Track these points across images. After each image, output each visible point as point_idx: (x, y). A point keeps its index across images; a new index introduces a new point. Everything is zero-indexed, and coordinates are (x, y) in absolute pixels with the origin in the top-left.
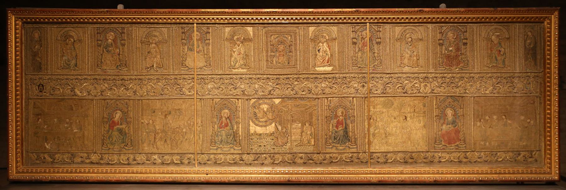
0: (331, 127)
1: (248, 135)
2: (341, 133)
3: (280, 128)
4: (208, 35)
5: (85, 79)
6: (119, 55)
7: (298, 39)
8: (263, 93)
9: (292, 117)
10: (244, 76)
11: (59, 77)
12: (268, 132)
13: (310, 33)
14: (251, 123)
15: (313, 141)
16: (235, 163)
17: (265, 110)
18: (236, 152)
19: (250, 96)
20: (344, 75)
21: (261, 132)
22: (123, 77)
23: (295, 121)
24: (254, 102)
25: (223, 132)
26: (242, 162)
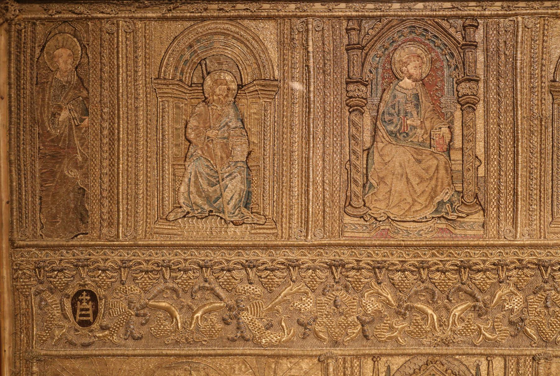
5: (291, 265)
6: (449, 149)
11: (168, 256)
22: (460, 257)
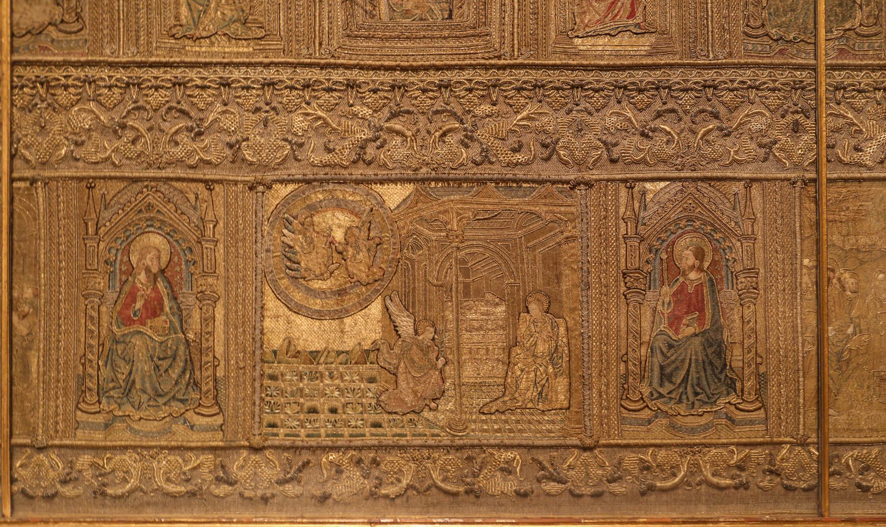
0: (646, 325)
1: (261, 359)
3: (405, 324)
9: (466, 273)
12: (349, 344)
14: (272, 303)
15: (561, 385)
16: (193, 494)
17: (339, 235)
18: (196, 439)
20: (709, 75)
23: (479, 294)
25: (137, 341)
26: (222, 490)
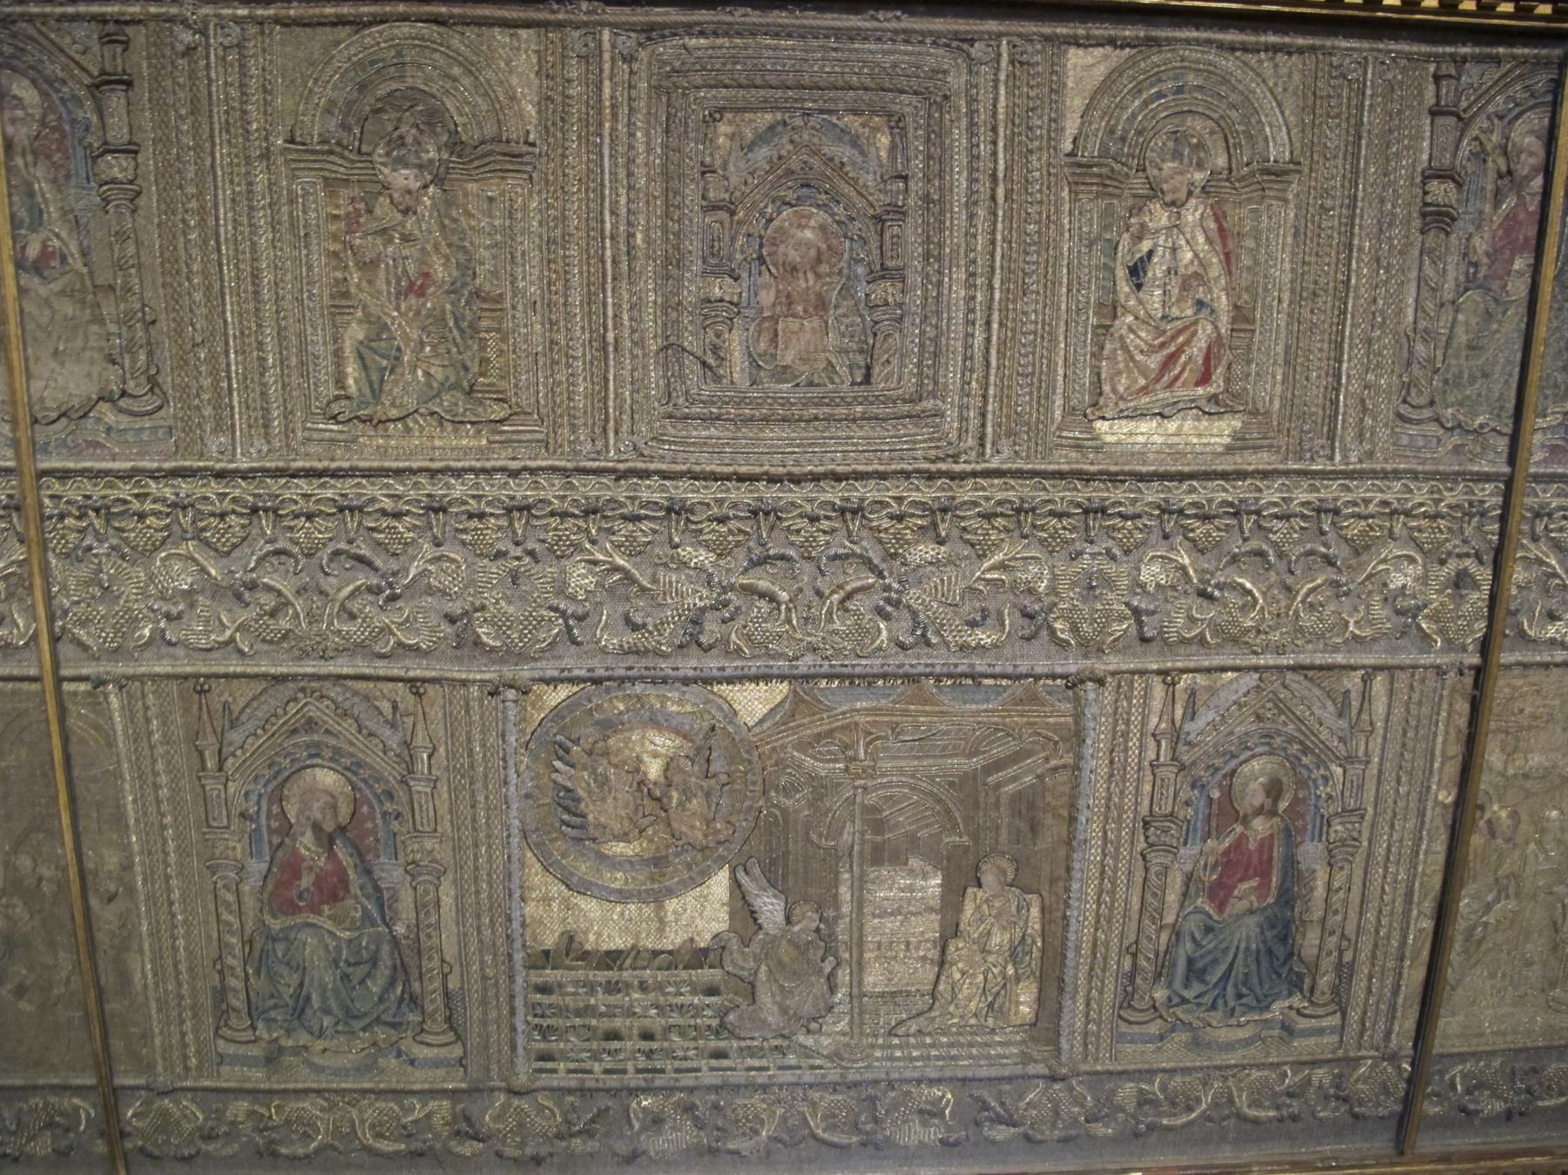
0: (1172, 898)
2: (1247, 933)
3: (770, 907)
4: (116, 101)
7: (960, 159)
8: (630, 638)
10: (458, 489)
12: (673, 939)
13: (1075, 103)
14: (536, 875)
17: (654, 769)
18: (419, 1079)
19: (522, 657)
20: (1331, 491)
21: (618, 942)
24: (557, 713)
26: (467, 1148)
